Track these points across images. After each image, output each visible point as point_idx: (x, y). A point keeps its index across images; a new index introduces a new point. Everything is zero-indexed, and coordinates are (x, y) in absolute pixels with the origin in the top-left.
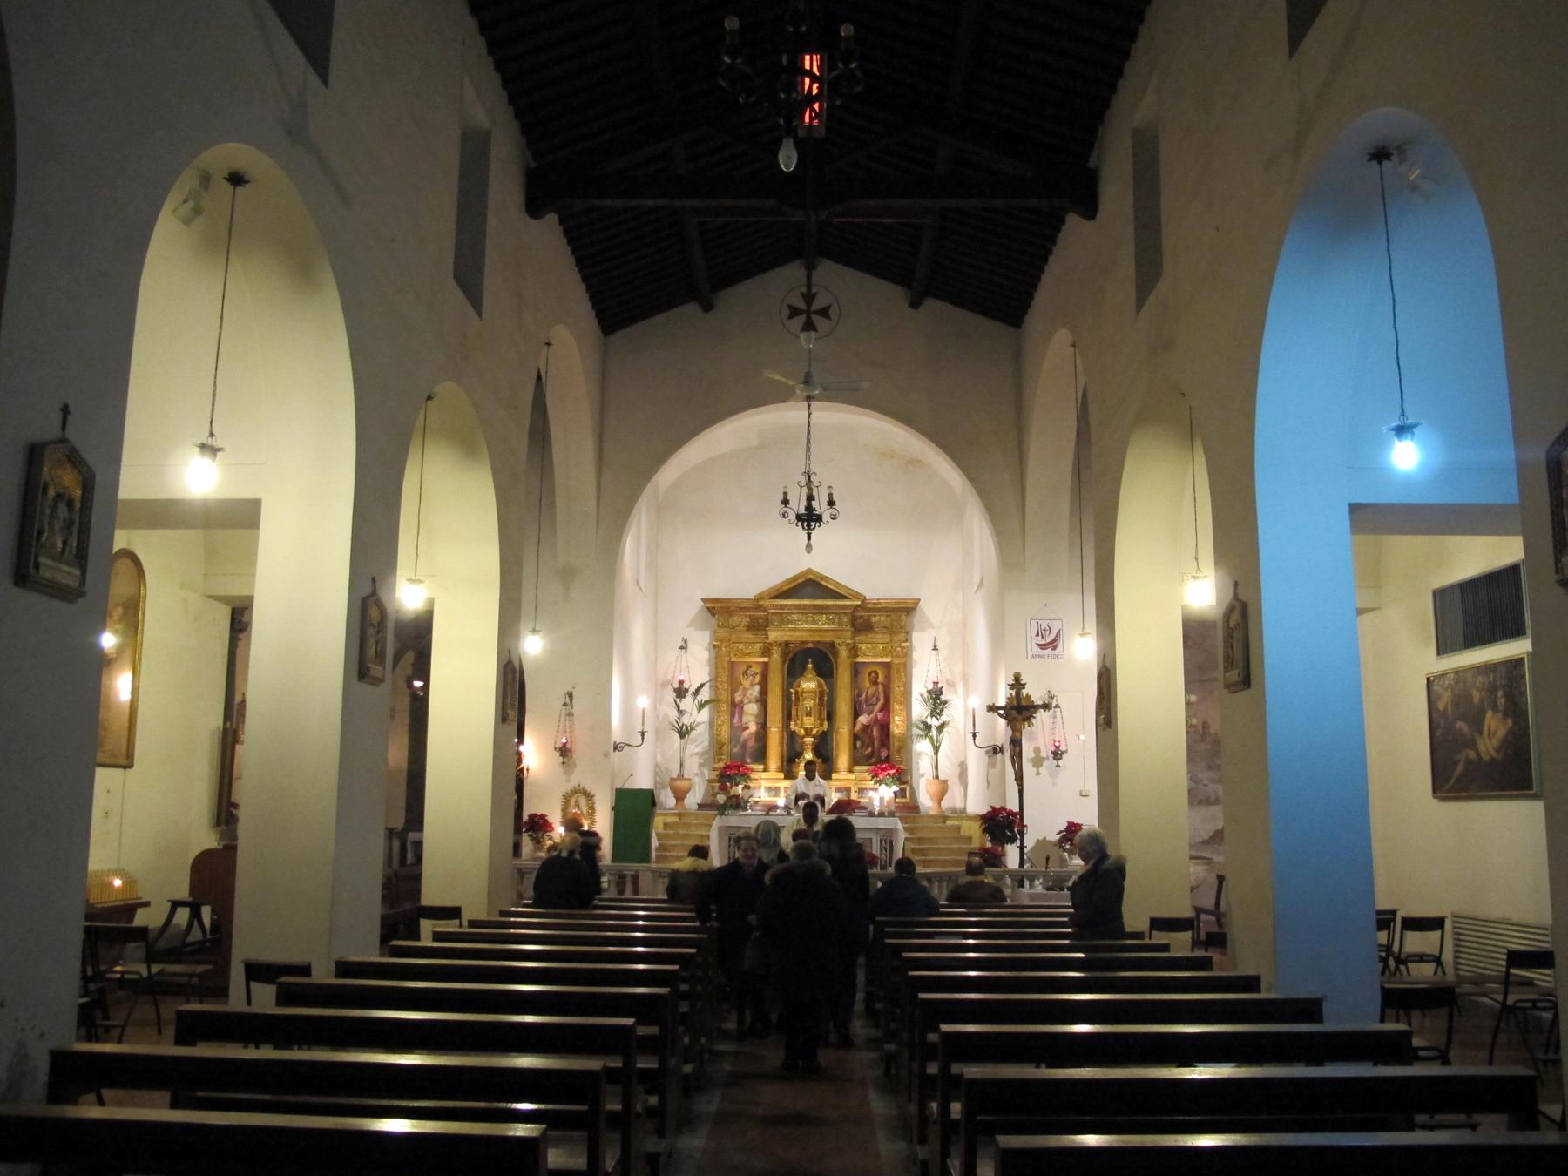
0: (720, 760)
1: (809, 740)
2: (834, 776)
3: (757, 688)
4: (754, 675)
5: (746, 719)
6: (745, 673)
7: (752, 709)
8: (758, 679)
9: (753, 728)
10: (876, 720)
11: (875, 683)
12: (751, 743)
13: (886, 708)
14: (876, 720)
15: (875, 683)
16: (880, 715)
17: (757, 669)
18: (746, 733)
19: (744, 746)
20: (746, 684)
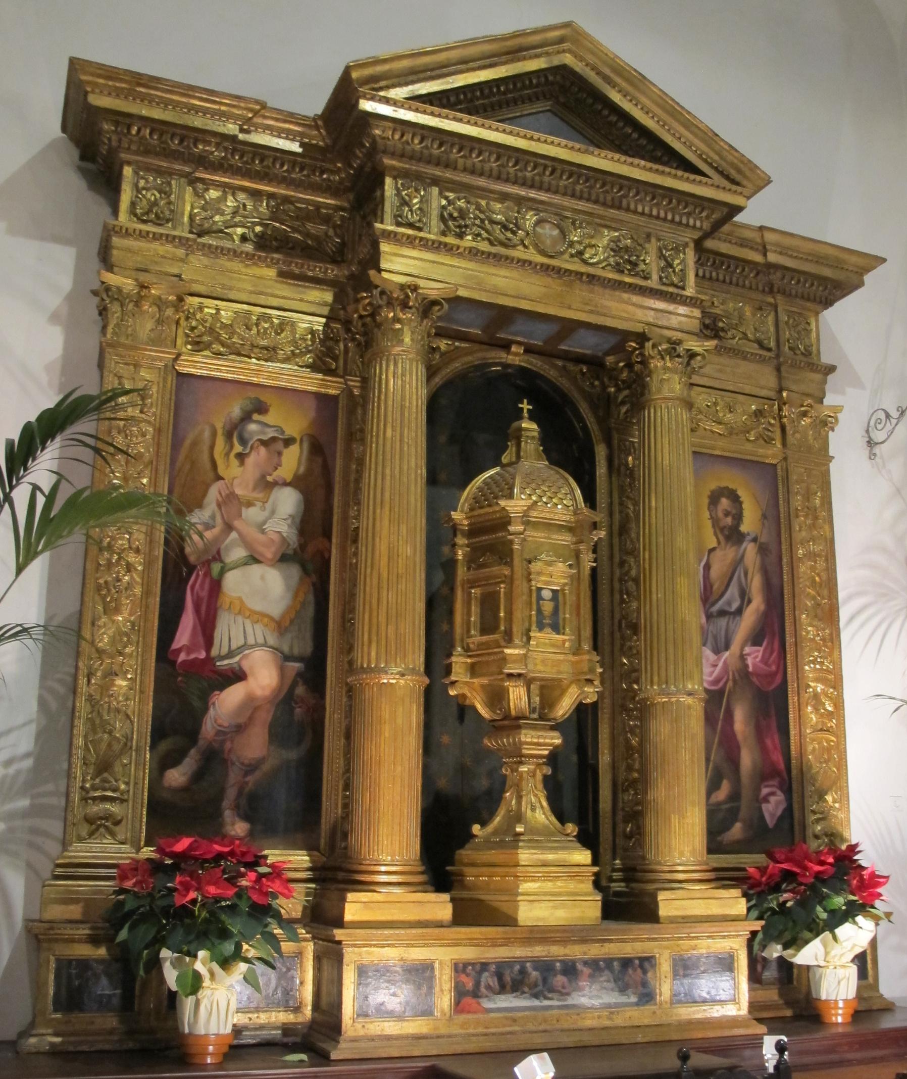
0: (99, 825)
1: (540, 742)
2: (668, 905)
3: (287, 502)
4: (276, 444)
5: (230, 631)
6: (235, 430)
7: (259, 592)
8: (292, 460)
9: (263, 676)
10: (744, 674)
11: (733, 535)
12: (255, 746)
13: (774, 629)
14: (744, 674)
15: (733, 535)
16: (754, 656)
17: (291, 422)
18: (229, 700)
19: (214, 760)
20: (239, 476)
